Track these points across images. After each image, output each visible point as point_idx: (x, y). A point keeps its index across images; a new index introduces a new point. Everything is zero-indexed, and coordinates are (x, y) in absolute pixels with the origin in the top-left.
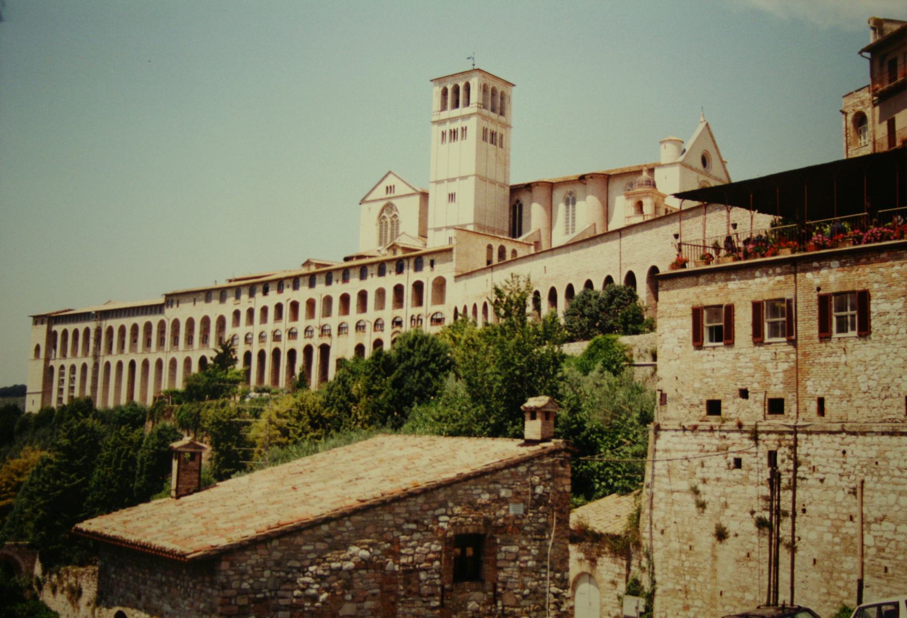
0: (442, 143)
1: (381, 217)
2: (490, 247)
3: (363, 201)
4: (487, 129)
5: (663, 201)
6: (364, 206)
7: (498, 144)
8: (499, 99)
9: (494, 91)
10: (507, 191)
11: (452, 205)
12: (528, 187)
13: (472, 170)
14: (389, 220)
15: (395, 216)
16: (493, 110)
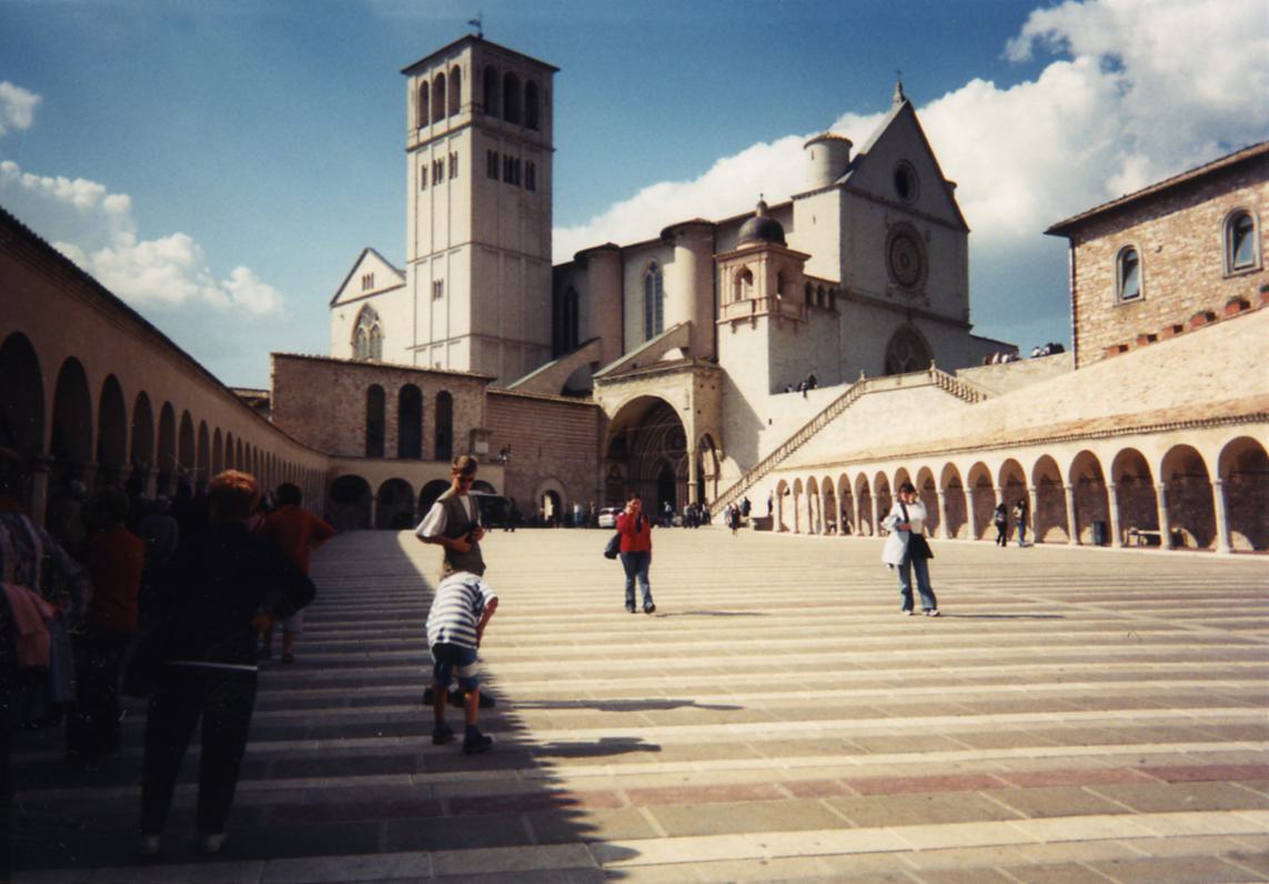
0: (423, 189)
1: (357, 331)
2: (376, 396)
3: (334, 303)
4: (496, 155)
5: (801, 267)
6: (337, 311)
7: (523, 182)
8: (523, 99)
9: (511, 81)
10: (549, 273)
11: (440, 304)
12: (583, 258)
13: (463, 231)
14: (367, 336)
15: (375, 327)
16: (510, 116)
